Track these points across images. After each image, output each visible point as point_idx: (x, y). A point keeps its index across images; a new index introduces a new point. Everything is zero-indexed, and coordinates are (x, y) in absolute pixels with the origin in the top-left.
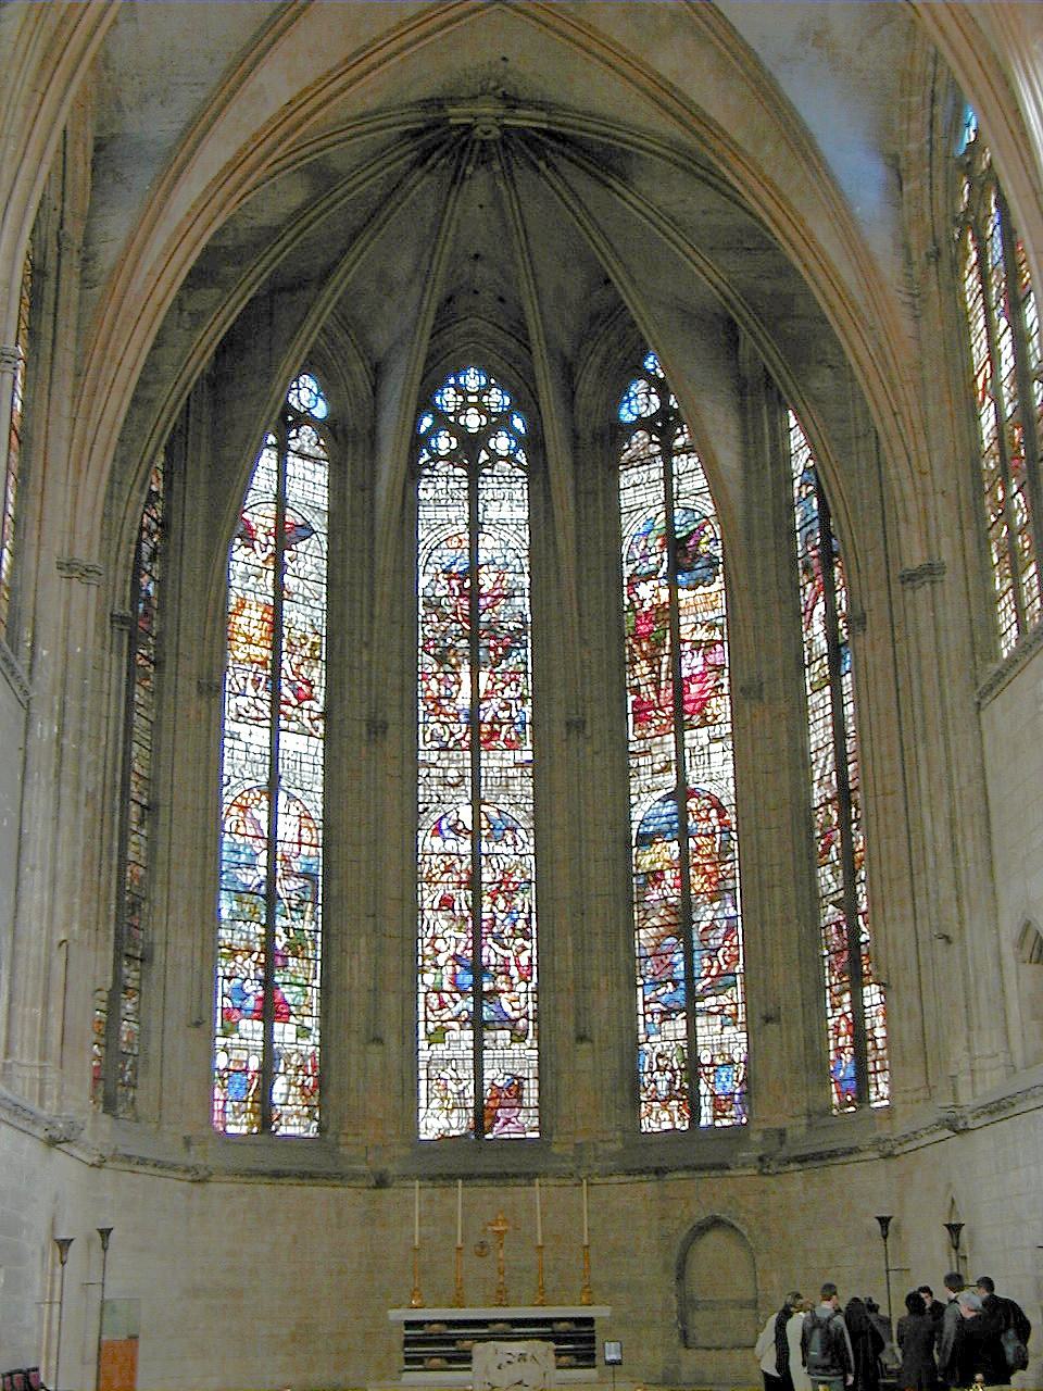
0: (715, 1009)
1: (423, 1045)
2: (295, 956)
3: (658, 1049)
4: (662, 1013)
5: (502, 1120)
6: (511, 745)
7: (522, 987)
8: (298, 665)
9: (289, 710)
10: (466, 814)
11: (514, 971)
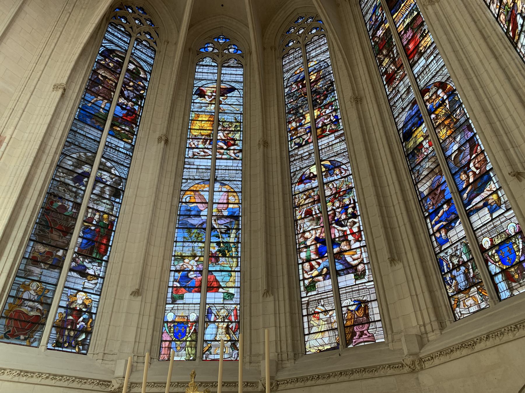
0: (481, 204)
1: (304, 294)
2: (224, 255)
3: (450, 251)
4: (443, 227)
5: (358, 333)
6: (332, 132)
7: (358, 245)
8: (228, 134)
9: (222, 151)
10: (314, 170)
11: (350, 238)
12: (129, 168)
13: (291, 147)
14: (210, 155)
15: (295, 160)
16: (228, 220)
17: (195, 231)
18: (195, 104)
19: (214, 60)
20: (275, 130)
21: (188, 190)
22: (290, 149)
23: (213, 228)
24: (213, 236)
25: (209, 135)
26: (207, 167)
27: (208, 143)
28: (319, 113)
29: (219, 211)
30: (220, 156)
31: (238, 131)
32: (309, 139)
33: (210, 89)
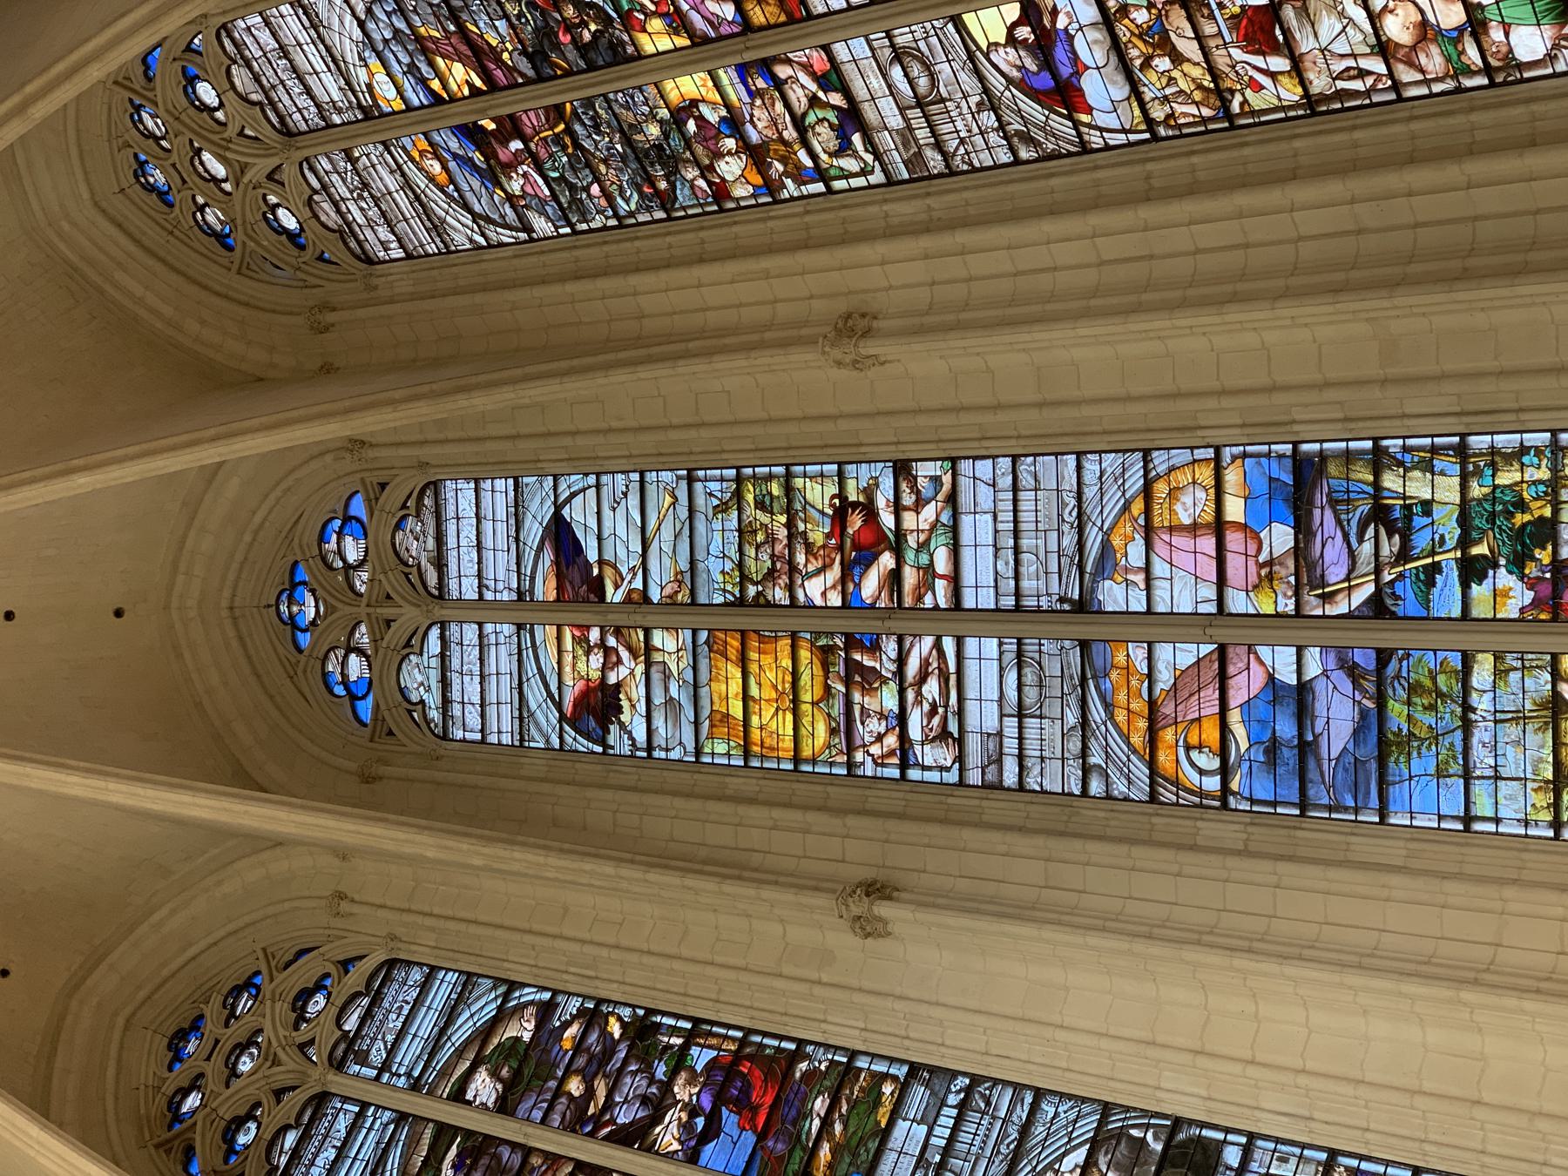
2: (1547, 531)
8: (809, 547)
9: (910, 577)
12: (1039, 1094)
13: (864, 172)
14: (938, 645)
15: (939, 146)
16: (1324, 519)
17: (1397, 711)
18: (659, 740)
19: (412, 645)
20: (767, 275)
21: (1152, 764)
22: (877, 177)
23: (1378, 607)
24: (1426, 603)
25: (825, 653)
26: (1010, 657)
27: (868, 662)
28: (656, 24)
29: (1267, 576)
30: (940, 585)
31: (789, 489)
32: (807, 68)
33: (568, 658)
